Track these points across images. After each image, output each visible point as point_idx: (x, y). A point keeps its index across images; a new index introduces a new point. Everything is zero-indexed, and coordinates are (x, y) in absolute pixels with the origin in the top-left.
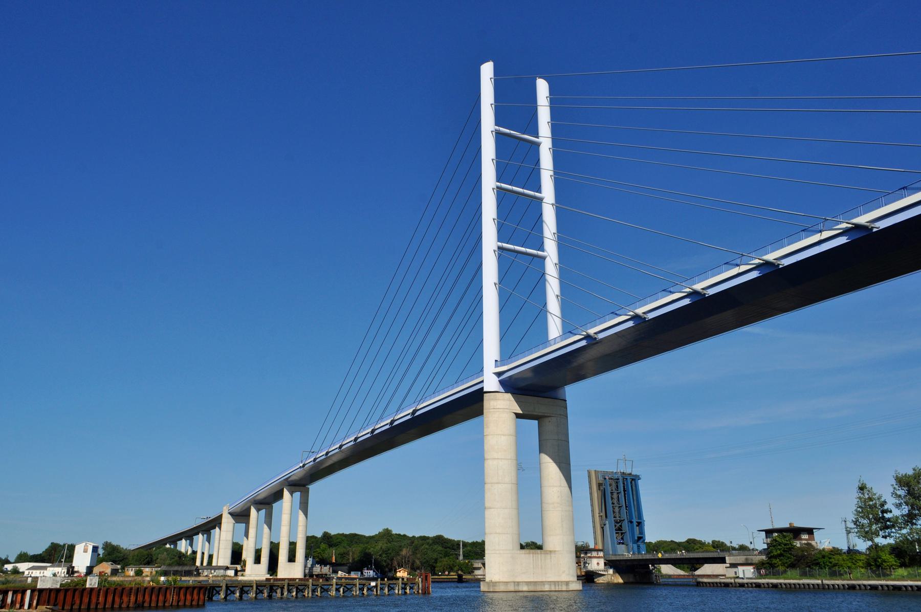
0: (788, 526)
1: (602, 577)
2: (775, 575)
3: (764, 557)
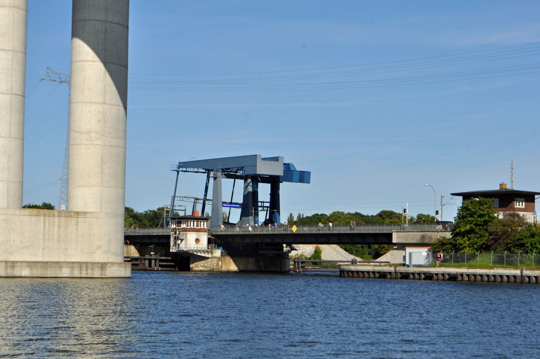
0: (497, 188)
1: (203, 262)
2: (458, 262)
3: (448, 235)
